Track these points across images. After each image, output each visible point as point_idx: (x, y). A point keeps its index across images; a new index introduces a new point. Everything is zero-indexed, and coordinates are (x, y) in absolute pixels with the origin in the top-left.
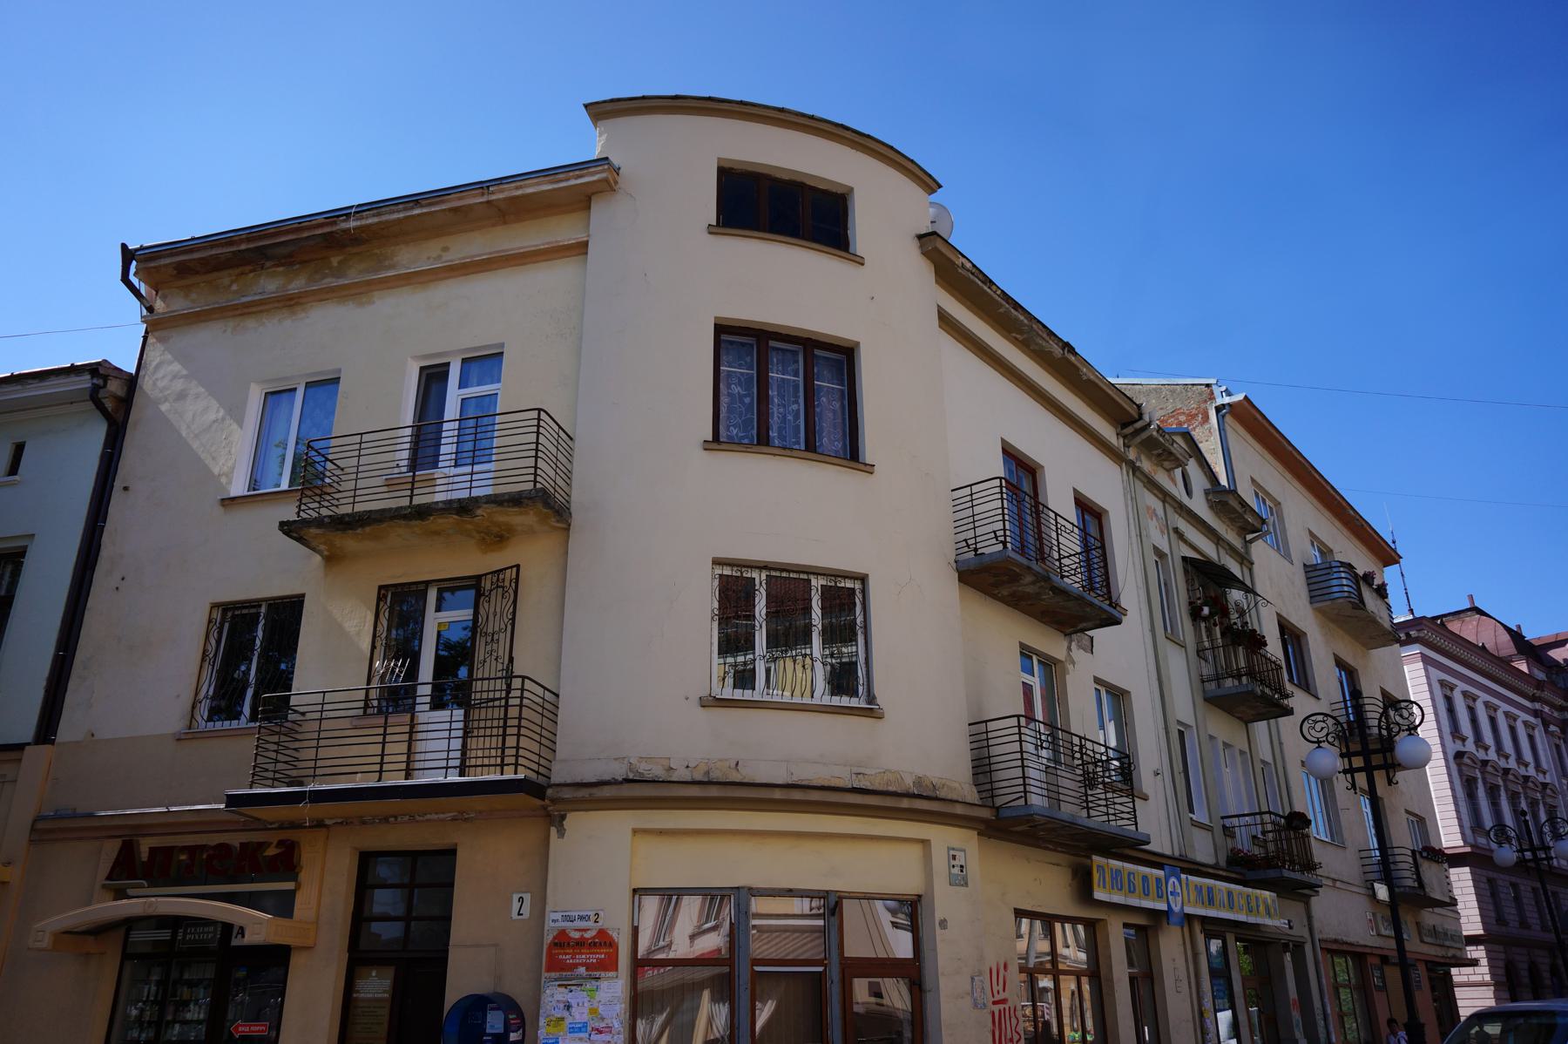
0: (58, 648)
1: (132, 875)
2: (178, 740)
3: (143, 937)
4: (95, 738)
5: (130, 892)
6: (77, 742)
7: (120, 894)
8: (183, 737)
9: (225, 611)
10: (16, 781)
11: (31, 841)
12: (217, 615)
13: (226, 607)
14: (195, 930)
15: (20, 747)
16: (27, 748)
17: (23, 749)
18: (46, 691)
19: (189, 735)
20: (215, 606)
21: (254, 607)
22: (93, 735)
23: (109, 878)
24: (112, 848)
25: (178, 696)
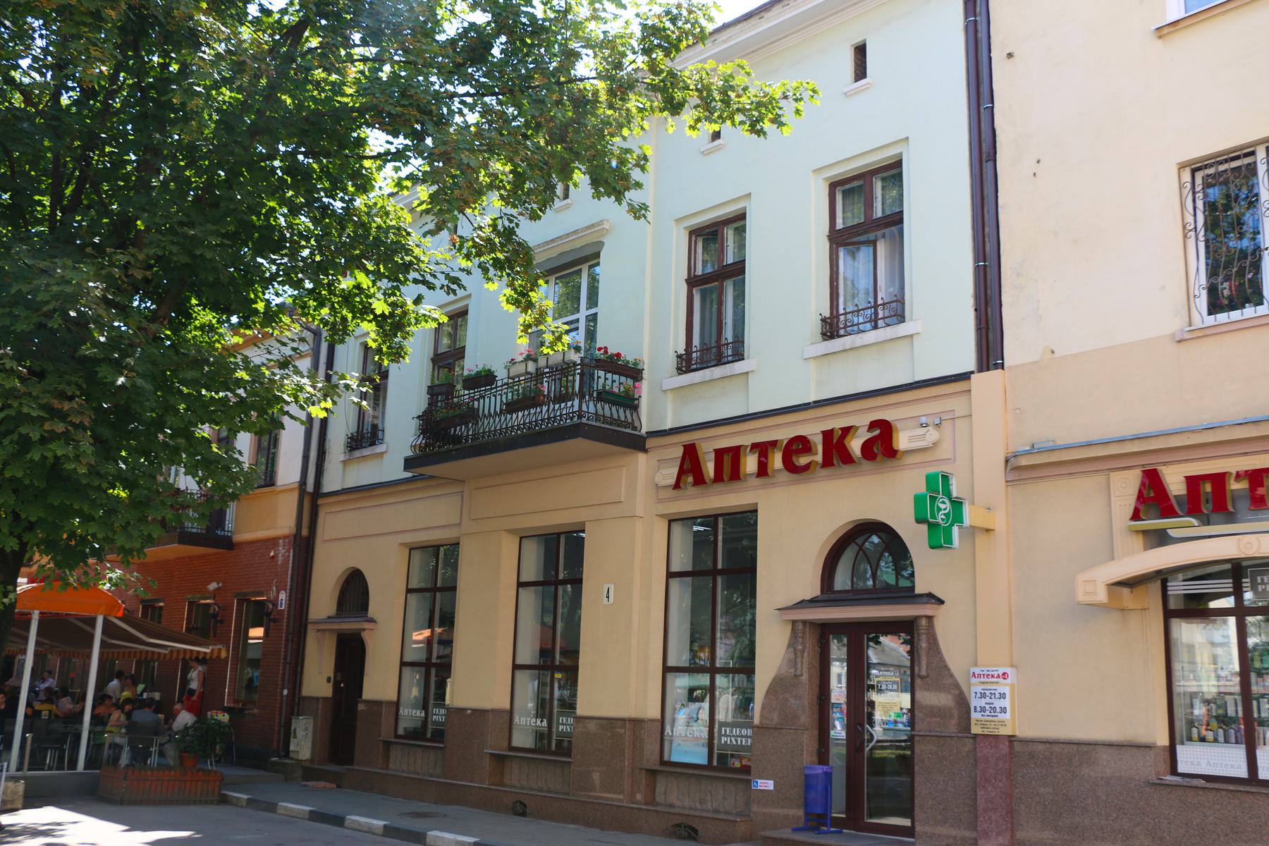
0: (976, 259)
1: (1168, 512)
2: (1179, 341)
3: (1178, 588)
4: (1056, 355)
5: (1173, 533)
6: (1034, 362)
7: (1160, 539)
8: (1187, 336)
9: (1193, 172)
10: (971, 415)
11: (1007, 481)
12: (1187, 176)
13: (1195, 167)
14: (1262, 580)
15: (965, 377)
16: (972, 375)
17: (969, 378)
18: (976, 310)
19: (1189, 337)
20: (1182, 166)
21: (1246, 155)
22: (1053, 352)
23: (1136, 516)
24: (1127, 486)
25: (1163, 288)
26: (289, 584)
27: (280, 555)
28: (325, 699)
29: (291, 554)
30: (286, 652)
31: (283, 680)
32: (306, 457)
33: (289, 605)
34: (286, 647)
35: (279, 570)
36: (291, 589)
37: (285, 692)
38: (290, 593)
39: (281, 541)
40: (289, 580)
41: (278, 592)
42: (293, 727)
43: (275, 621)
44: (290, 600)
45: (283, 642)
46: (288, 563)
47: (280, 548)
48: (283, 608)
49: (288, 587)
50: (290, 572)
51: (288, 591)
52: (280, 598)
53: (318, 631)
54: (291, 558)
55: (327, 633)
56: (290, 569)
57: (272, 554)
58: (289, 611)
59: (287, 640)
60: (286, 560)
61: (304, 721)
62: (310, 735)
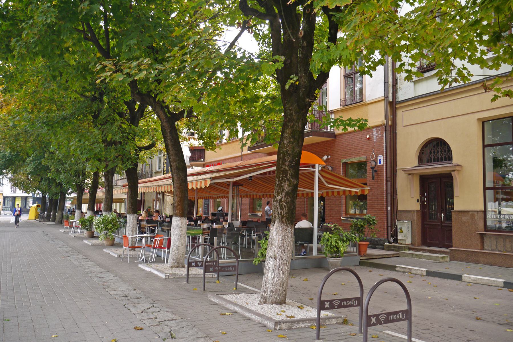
26: (384, 151)
27: (375, 137)
28: (417, 211)
29: (384, 135)
30: (387, 187)
31: (387, 202)
32: (386, 82)
33: (386, 162)
34: (387, 184)
35: (375, 144)
36: (386, 154)
37: (389, 208)
38: (386, 156)
39: (374, 129)
40: (384, 149)
41: (376, 156)
42: (398, 227)
43: (376, 171)
44: (386, 159)
45: (385, 182)
46: (382, 139)
47: (374, 133)
48: (382, 164)
49: (385, 153)
50: (384, 145)
51: (385, 155)
52: (378, 158)
53: (409, 174)
54: (384, 137)
55: (415, 175)
56: (384, 143)
57: (368, 137)
58: (386, 165)
59: (387, 181)
60: (380, 139)
61: (407, 223)
62: (410, 231)
